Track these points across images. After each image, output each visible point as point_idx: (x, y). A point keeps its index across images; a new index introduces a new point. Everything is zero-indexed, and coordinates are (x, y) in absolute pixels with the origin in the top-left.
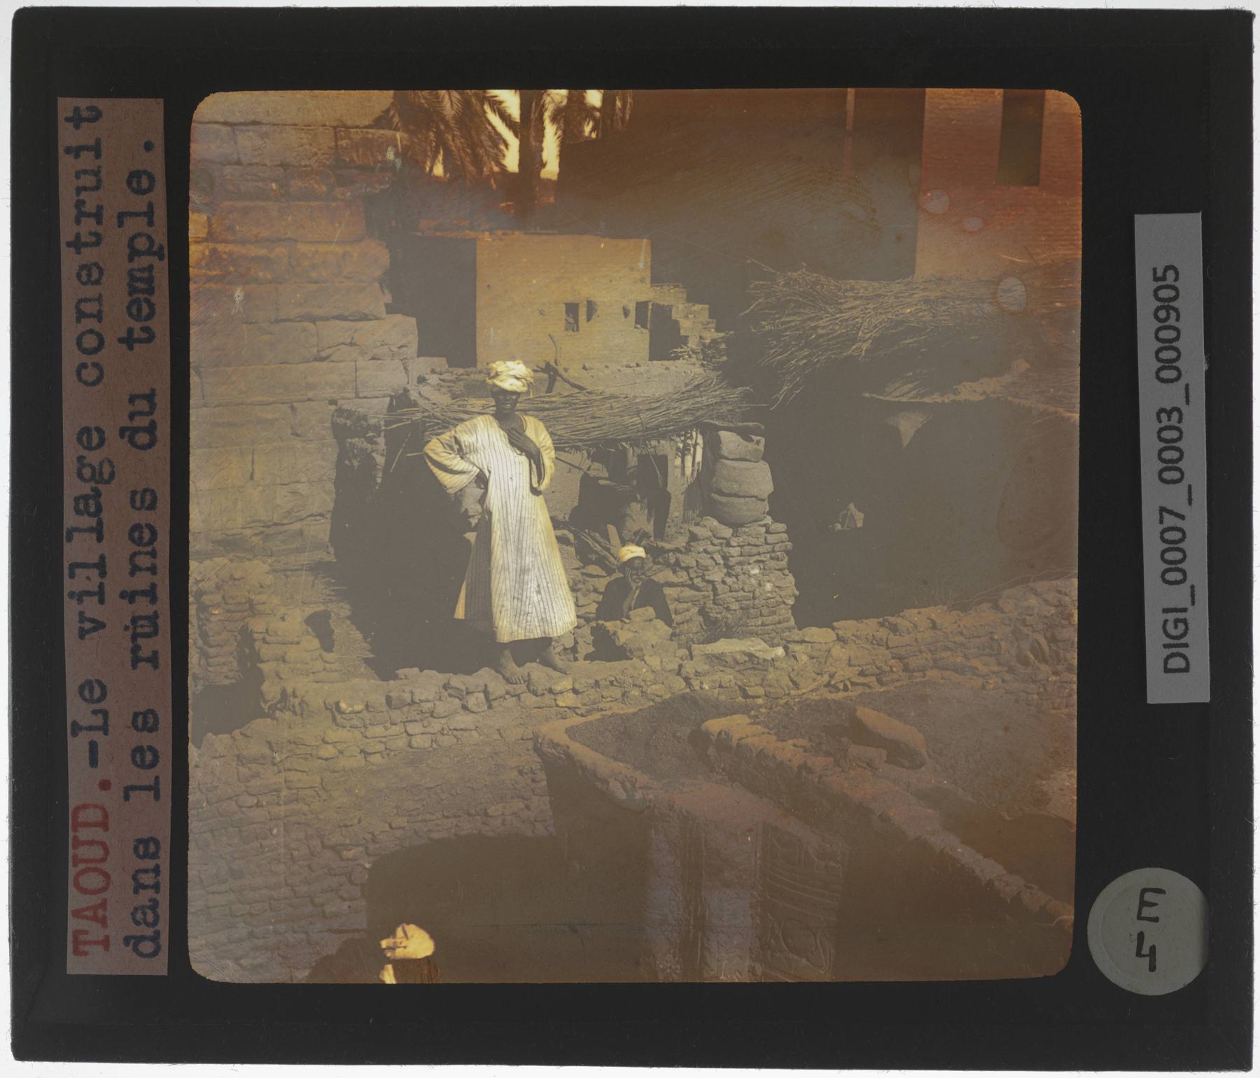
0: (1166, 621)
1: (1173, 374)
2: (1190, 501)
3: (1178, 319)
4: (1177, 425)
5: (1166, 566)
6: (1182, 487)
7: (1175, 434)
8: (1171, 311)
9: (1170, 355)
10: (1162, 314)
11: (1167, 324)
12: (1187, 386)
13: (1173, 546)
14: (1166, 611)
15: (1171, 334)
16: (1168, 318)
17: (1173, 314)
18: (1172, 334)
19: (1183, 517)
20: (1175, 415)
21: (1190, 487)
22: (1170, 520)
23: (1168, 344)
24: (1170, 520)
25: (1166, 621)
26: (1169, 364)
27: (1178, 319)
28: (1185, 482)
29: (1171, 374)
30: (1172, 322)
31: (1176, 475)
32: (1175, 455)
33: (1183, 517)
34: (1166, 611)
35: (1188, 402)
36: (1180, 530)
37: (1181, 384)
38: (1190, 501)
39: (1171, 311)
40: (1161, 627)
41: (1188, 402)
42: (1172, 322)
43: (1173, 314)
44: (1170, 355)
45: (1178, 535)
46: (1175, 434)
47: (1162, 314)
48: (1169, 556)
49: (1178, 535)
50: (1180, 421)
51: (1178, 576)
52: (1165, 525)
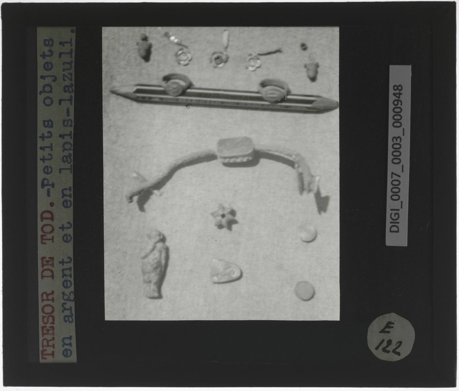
0: (392, 214)
1: (398, 124)
2: (403, 171)
3: (401, 105)
4: (399, 143)
5: (392, 194)
6: (400, 165)
7: (398, 146)
8: (399, 102)
9: (398, 117)
10: (396, 103)
11: (397, 106)
12: (404, 129)
13: (395, 186)
14: (392, 210)
15: (398, 110)
16: (398, 104)
17: (400, 103)
18: (398, 110)
19: (399, 176)
20: (399, 139)
21: (403, 166)
22: (395, 177)
23: (398, 114)
24: (395, 177)
25: (392, 214)
26: (397, 121)
27: (401, 105)
28: (401, 164)
29: (398, 124)
30: (399, 106)
31: (398, 161)
32: (398, 154)
33: (399, 176)
34: (392, 210)
35: (403, 135)
36: (400, 182)
37: (402, 128)
38: (403, 171)
39: (399, 102)
40: (390, 216)
41: (403, 135)
42: (399, 106)
43: (400, 103)
44: (398, 117)
45: (397, 183)
46: (398, 146)
47: (396, 103)
48: (394, 190)
49: (397, 183)
50: (401, 141)
51: (397, 197)
52: (393, 179)
